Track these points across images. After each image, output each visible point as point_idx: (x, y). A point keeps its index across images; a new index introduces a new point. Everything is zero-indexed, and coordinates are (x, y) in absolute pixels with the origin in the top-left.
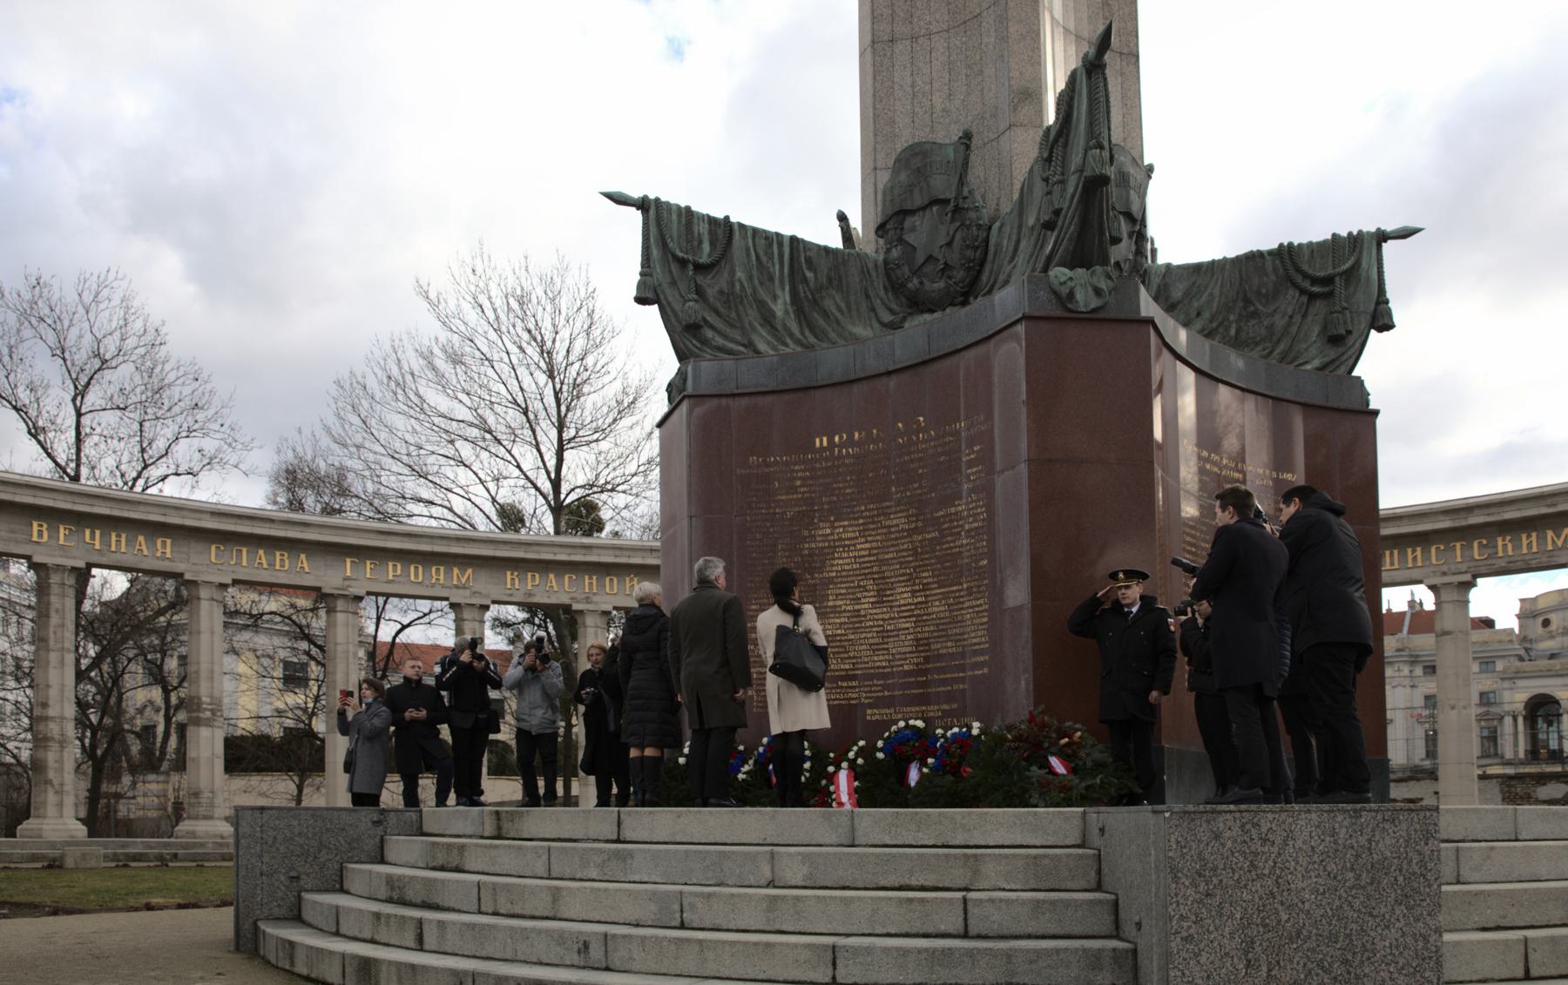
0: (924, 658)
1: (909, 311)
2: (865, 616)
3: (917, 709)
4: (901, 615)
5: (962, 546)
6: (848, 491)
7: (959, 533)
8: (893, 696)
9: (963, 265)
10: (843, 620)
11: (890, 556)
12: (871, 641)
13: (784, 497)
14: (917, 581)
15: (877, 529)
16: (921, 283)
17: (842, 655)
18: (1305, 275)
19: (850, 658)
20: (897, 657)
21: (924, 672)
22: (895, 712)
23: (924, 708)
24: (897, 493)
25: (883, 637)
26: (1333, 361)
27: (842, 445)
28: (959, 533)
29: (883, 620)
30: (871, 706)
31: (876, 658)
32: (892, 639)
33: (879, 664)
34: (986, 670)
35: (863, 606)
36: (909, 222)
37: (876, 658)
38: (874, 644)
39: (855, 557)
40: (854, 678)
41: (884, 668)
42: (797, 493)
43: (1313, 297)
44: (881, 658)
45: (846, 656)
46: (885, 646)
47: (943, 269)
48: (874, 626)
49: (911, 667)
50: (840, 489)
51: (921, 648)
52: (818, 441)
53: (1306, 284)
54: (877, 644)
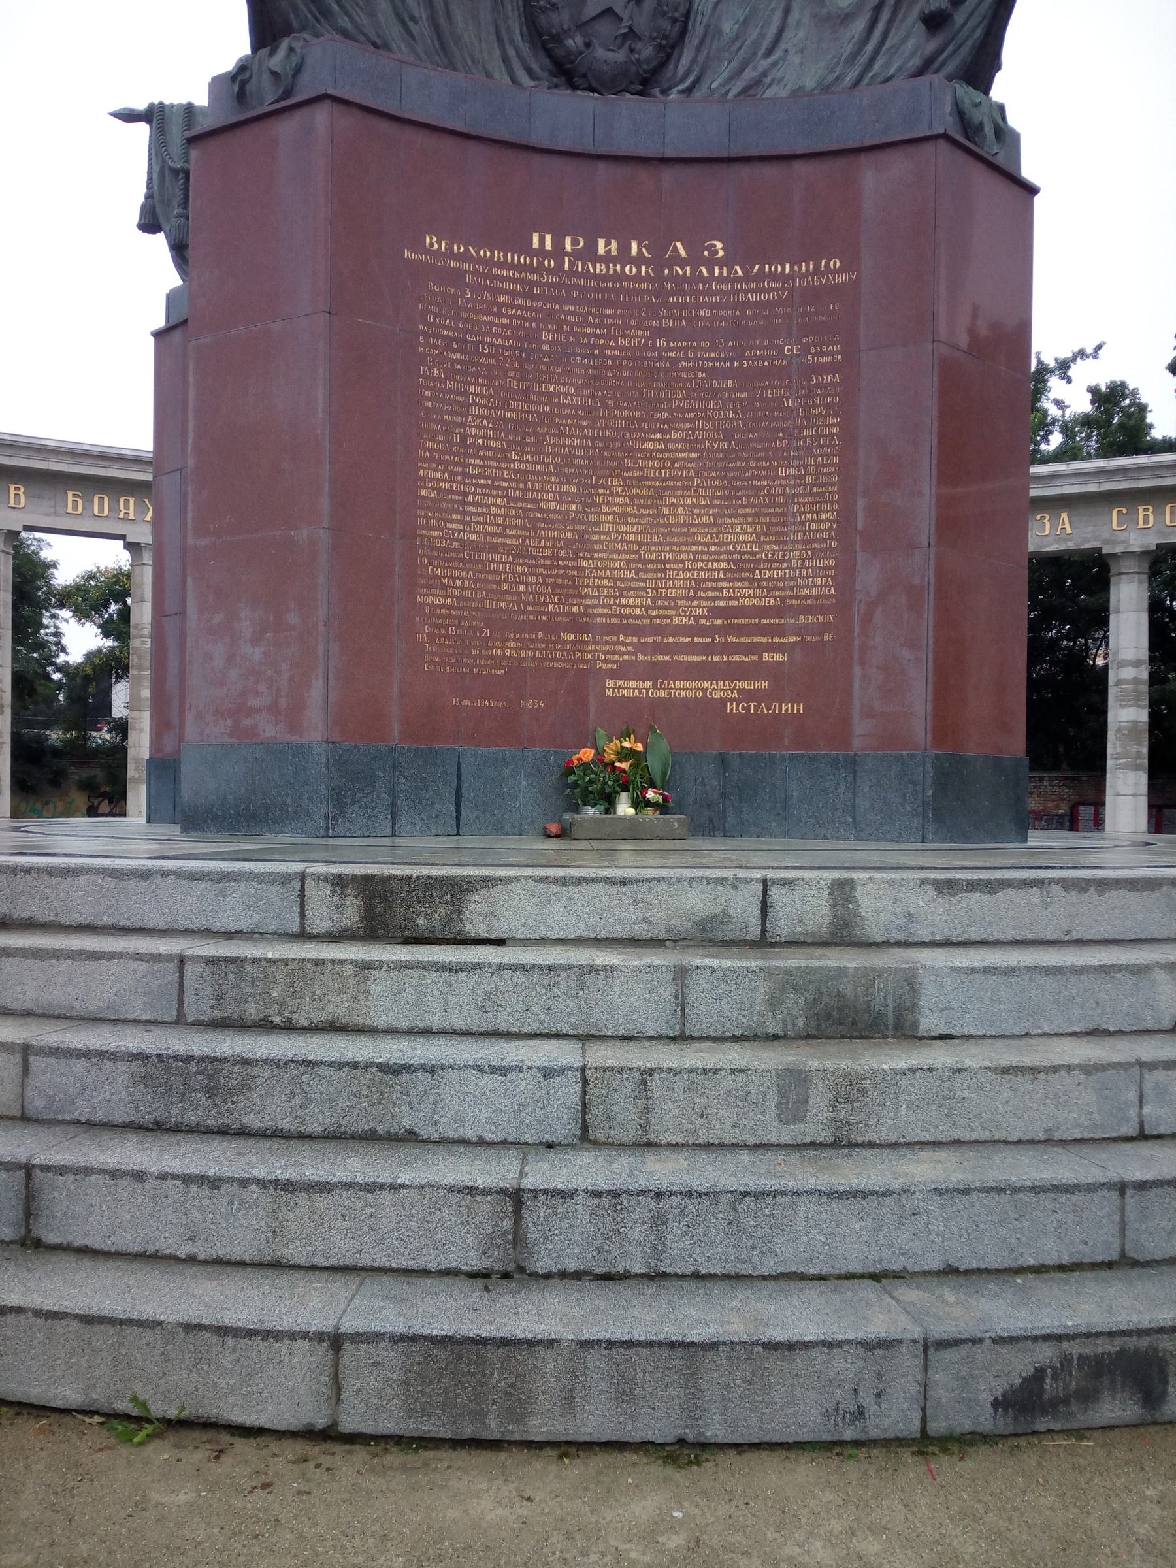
0: (710, 609)
2: (608, 533)
3: (695, 684)
4: (669, 539)
6: (584, 330)
9: (654, 39)
11: (655, 446)
12: (620, 574)
13: (479, 317)
14: (702, 492)
16: (588, 45)
19: (582, 597)
20: (660, 603)
22: (655, 687)
23: (707, 684)
24: (670, 349)
25: (637, 571)
27: (576, 255)
29: (640, 544)
30: (613, 675)
31: (623, 601)
33: (628, 611)
34: (828, 637)
35: (605, 518)
37: (623, 601)
38: (622, 580)
39: (593, 439)
42: (499, 314)
44: (631, 601)
45: (571, 592)
46: (642, 585)
48: (624, 552)
49: (686, 620)
50: (572, 324)
51: (701, 594)
54: (627, 580)
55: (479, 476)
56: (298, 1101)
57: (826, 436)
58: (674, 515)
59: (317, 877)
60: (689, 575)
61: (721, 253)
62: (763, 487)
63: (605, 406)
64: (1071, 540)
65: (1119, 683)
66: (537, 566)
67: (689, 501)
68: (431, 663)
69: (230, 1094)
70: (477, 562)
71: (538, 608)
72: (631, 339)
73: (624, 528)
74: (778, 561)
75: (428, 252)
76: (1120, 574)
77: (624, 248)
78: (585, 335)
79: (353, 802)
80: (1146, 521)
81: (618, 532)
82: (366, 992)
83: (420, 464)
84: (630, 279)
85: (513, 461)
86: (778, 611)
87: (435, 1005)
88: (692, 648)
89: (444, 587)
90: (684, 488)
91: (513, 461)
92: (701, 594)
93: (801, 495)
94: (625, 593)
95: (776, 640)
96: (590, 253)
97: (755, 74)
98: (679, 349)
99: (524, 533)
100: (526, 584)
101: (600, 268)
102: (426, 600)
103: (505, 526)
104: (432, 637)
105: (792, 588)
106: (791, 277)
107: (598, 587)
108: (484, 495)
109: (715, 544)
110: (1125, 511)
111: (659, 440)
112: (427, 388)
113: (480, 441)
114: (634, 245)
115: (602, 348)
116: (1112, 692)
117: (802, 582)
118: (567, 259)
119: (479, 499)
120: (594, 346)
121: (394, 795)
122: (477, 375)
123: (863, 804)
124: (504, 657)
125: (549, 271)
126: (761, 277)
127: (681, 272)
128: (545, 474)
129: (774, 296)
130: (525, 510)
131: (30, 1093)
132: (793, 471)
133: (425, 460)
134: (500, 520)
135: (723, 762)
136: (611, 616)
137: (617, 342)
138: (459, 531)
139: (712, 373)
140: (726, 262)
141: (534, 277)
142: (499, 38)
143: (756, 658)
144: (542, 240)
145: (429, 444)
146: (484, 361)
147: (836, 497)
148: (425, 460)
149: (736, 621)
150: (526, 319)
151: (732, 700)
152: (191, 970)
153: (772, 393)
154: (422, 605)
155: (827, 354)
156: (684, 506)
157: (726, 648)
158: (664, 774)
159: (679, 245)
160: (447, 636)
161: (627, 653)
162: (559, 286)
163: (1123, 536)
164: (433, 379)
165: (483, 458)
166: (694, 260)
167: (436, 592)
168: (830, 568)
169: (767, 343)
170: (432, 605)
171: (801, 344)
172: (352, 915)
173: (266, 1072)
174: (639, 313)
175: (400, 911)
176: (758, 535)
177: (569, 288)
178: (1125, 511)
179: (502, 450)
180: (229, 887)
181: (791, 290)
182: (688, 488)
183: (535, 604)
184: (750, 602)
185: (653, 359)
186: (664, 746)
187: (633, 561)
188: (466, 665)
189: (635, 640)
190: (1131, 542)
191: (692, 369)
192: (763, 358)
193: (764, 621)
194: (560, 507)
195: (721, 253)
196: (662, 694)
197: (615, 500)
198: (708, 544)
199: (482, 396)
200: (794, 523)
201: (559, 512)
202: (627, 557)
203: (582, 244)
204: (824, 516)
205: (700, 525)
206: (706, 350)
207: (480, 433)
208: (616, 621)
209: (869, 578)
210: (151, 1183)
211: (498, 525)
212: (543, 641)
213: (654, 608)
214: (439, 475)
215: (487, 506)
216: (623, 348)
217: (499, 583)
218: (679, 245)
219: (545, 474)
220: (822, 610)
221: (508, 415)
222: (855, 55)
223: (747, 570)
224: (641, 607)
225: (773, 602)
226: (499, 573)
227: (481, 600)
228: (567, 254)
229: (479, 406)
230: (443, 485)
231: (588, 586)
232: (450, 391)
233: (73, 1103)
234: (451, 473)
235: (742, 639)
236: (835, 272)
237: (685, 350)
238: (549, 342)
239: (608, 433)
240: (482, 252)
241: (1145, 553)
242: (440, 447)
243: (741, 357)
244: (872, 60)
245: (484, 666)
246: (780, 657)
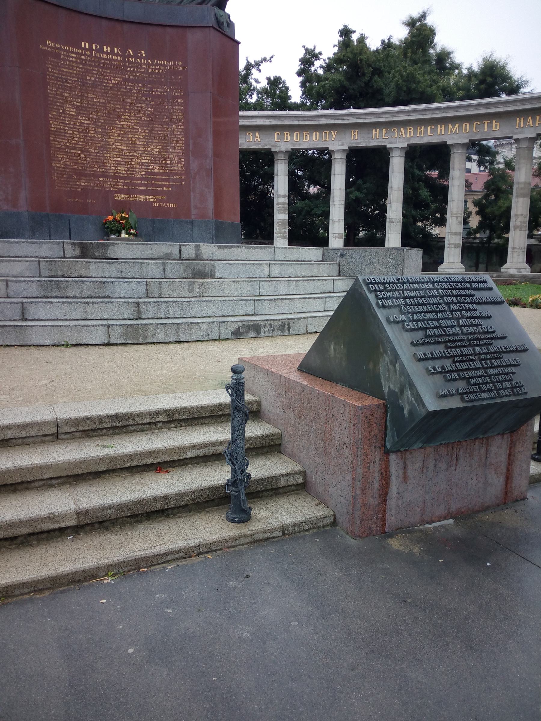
2: (112, 145)
3: (143, 197)
8: (129, 189)
14: (142, 134)
20: (130, 169)
22: (130, 197)
23: (147, 197)
24: (129, 86)
27: (97, 51)
29: (123, 150)
30: (117, 192)
31: (118, 168)
32: (127, 160)
34: (183, 183)
35: (111, 140)
37: (118, 168)
38: (118, 161)
39: (106, 114)
41: (123, 174)
44: (121, 168)
45: (101, 164)
46: (124, 163)
48: (118, 152)
49: (139, 176)
50: (96, 74)
51: (143, 167)
55: (69, 124)
56: (81, 290)
57: (179, 119)
58: (133, 141)
59: (67, 243)
60: (139, 161)
61: (144, 55)
62: (161, 134)
63: (109, 103)
64: (260, 144)
65: (278, 204)
66: (89, 155)
67: (138, 137)
68: (58, 186)
69: (63, 289)
70: (70, 153)
71: (91, 169)
72: (116, 81)
73: (117, 144)
74: (167, 158)
76: (278, 160)
77: (112, 50)
78: (101, 78)
79: (37, 231)
80: (287, 139)
81: (116, 145)
82: (89, 268)
83: (50, 119)
85: (80, 119)
86: (168, 174)
87: (106, 271)
88: (142, 185)
89: (60, 161)
90: (136, 132)
91: (80, 119)
92: (143, 167)
93: (173, 137)
94: (119, 165)
95: (167, 183)
96: (101, 51)
98: (132, 86)
99: (85, 144)
100: (86, 161)
102: (55, 165)
103: (78, 141)
104: (57, 177)
105: (171, 167)
106: (166, 66)
107: (110, 163)
108: (71, 130)
109: (147, 151)
110: (279, 134)
111: (127, 116)
112: (51, 94)
113: (69, 112)
114: (116, 49)
115: (107, 83)
116: (276, 207)
117: (174, 165)
118: (94, 52)
120: (104, 83)
121: (49, 229)
122: (66, 90)
123: (195, 235)
124: (81, 185)
125: (88, 56)
126: (157, 64)
127: (131, 60)
128: (90, 124)
130: (85, 136)
131: (9, 291)
132: (170, 129)
133: (51, 118)
135: (153, 222)
136: (115, 173)
137: (111, 82)
138: (64, 142)
139: (143, 95)
140: (146, 58)
141: (83, 57)
143: (161, 189)
145: (52, 113)
146: (68, 85)
147: (183, 139)
148: (51, 118)
149: (155, 177)
150: (81, 72)
151: (155, 202)
152: (42, 264)
153: (162, 103)
154: (54, 167)
155: (179, 93)
156: (136, 138)
157: (152, 185)
158: (135, 225)
159: (130, 51)
160: (62, 177)
161: (120, 185)
162: (92, 61)
163: (279, 144)
164: (52, 90)
165: (70, 118)
166: (135, 56)
167: (58, 162)
168: (183, 161)
169: (160, 87)
170: (57, 167)
171: (171, 88)
172: (77, 252)
173: (72, 283)
174: (119, 72)
175: (91, 251)
176: (160, 149)
177: (95, 62)
178: (279, 134)
179: (76, 116)
180: (43, 245)
181: (167, 70)
182: (137, 132)
183: (90, 168)
184: (159, 171)
185: (124, 88)
186: (134, 216)
187: (121, 155)
188: (69, 187)
190: (282, 147)
191: (137, 93)
192: (159, 92)
193: (163, 177)
195: (144, 55)
196: (133, 199)
197: (114, 134)
198: (144, 151)
199: (69, 97)
200: (171, 146)
201: (96, 137)
202: (119, 154)
203: (98, 47)
204: (180, 145)
205: (142, 145)
206: (140, 87)
207: (69, 109)
208: (117, 175)
209: (194, 165)
210: (54, 304)
211: (76, 141)
212: (93, 180)
213: (128, 171)
214: (56, 123)
215: (73, 134)
216: (114, 84)
217: (78, 160)
218: (130, 51)
219: (90, 124)
220: (181, 175)
221: (77, 104)
223: (157, 160)
224: (124, 170)
225: (166, 171)
226: (78, 157)
227: (72, 166)
228: (94, 50)
229: (68, 100)
230: (58, 127)
231: (107, 163)
233: (22, 293)
234: (60, 123)
235: (157, 183)
236: (180, 66)
237: (134, 86)
238: (89, 80)
239: (110, 112)
240: (66, 48)
241: (287, 152)
242: (56, 114)
243: (152, 91)
245: (75, 188)
246: (169, 189)
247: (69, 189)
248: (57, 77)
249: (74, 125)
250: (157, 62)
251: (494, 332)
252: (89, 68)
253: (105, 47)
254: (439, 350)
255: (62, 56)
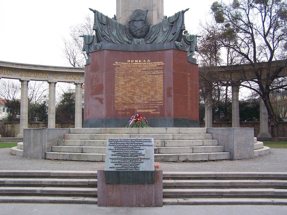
1: (133, 37)
3: (147, 110)
5: (157, 83)
7: (157, 81)
10: (132, 93)
11: (142, 83)
15: (140, 78)
17: (132, 100)
18: (187, 41)
21: (149, 104)
26: (191, 55)
27: (133, 62)
28: (157, 81)
34: (162, 104)
36: (135, 22)
39: (135, 82)
40: (134, 104)
43: (188, 44)
47: (141, 32)
52: (128, 61)
53: (187, 42)
61: (149, 61)
62: (154, 87)
75: (116, 64)
77: (138, 61)
84: (139, 65)
86: (157, 102)
96: (134, 62)
97: (156, 37)
101: (136, 63)
102: (115, 102)
114: (139, 60)
115: (136, 72)
119: (122, 90)
126: (154, 64)
129: (155, 66)
132: (158, 86)
133: (115, 86)
134: (124, 92)
139: (149, 75)
141: (128, 65)
142: (126, 33)
144: (129, 61)
146: (122, 75)
153: (155, 77)
157: (151, 106)
160: (118, 105)
162: (131, 66)
166: (146, 62)
170: (116, 102)
177: (132, 66)
189: (140, 105)
194: (132, 90)
207: (122, 83)
214: (117, 88)
218: (145, 60)
220: (162, 101)
222: (166, 37)
232: (119, 79)
239: (137, 82)
242: (117, 85)
244: (168, 37)
246: (157, 107)
247: (120, 109)
248: (118, 73)
249: (123, 88)
250: (154, 63)
251: (141, 153)
252: (129, 68)
253: (136, 61)
254: (120, 157)
255: (120, 66)
